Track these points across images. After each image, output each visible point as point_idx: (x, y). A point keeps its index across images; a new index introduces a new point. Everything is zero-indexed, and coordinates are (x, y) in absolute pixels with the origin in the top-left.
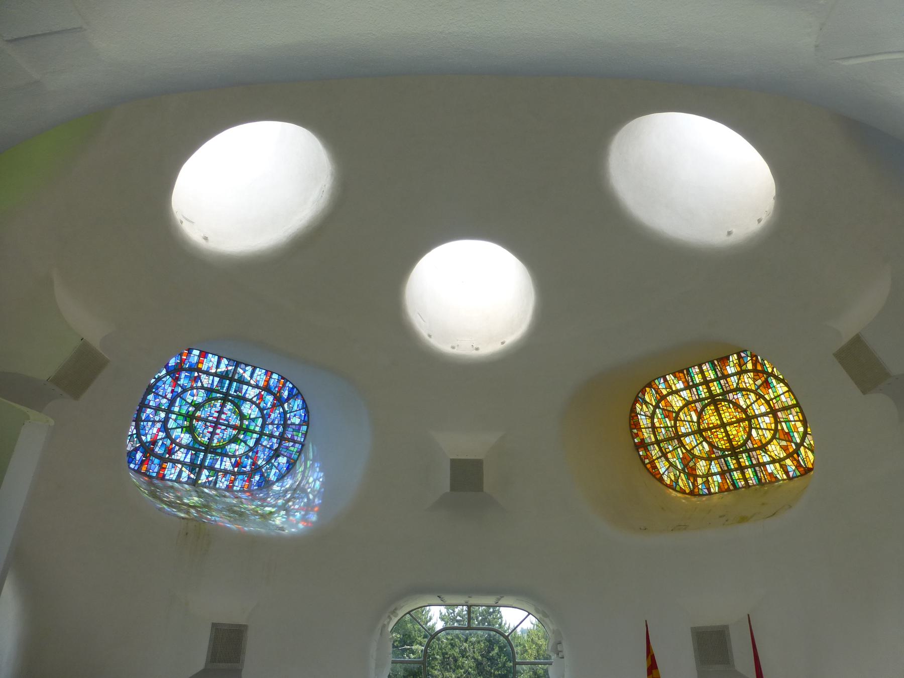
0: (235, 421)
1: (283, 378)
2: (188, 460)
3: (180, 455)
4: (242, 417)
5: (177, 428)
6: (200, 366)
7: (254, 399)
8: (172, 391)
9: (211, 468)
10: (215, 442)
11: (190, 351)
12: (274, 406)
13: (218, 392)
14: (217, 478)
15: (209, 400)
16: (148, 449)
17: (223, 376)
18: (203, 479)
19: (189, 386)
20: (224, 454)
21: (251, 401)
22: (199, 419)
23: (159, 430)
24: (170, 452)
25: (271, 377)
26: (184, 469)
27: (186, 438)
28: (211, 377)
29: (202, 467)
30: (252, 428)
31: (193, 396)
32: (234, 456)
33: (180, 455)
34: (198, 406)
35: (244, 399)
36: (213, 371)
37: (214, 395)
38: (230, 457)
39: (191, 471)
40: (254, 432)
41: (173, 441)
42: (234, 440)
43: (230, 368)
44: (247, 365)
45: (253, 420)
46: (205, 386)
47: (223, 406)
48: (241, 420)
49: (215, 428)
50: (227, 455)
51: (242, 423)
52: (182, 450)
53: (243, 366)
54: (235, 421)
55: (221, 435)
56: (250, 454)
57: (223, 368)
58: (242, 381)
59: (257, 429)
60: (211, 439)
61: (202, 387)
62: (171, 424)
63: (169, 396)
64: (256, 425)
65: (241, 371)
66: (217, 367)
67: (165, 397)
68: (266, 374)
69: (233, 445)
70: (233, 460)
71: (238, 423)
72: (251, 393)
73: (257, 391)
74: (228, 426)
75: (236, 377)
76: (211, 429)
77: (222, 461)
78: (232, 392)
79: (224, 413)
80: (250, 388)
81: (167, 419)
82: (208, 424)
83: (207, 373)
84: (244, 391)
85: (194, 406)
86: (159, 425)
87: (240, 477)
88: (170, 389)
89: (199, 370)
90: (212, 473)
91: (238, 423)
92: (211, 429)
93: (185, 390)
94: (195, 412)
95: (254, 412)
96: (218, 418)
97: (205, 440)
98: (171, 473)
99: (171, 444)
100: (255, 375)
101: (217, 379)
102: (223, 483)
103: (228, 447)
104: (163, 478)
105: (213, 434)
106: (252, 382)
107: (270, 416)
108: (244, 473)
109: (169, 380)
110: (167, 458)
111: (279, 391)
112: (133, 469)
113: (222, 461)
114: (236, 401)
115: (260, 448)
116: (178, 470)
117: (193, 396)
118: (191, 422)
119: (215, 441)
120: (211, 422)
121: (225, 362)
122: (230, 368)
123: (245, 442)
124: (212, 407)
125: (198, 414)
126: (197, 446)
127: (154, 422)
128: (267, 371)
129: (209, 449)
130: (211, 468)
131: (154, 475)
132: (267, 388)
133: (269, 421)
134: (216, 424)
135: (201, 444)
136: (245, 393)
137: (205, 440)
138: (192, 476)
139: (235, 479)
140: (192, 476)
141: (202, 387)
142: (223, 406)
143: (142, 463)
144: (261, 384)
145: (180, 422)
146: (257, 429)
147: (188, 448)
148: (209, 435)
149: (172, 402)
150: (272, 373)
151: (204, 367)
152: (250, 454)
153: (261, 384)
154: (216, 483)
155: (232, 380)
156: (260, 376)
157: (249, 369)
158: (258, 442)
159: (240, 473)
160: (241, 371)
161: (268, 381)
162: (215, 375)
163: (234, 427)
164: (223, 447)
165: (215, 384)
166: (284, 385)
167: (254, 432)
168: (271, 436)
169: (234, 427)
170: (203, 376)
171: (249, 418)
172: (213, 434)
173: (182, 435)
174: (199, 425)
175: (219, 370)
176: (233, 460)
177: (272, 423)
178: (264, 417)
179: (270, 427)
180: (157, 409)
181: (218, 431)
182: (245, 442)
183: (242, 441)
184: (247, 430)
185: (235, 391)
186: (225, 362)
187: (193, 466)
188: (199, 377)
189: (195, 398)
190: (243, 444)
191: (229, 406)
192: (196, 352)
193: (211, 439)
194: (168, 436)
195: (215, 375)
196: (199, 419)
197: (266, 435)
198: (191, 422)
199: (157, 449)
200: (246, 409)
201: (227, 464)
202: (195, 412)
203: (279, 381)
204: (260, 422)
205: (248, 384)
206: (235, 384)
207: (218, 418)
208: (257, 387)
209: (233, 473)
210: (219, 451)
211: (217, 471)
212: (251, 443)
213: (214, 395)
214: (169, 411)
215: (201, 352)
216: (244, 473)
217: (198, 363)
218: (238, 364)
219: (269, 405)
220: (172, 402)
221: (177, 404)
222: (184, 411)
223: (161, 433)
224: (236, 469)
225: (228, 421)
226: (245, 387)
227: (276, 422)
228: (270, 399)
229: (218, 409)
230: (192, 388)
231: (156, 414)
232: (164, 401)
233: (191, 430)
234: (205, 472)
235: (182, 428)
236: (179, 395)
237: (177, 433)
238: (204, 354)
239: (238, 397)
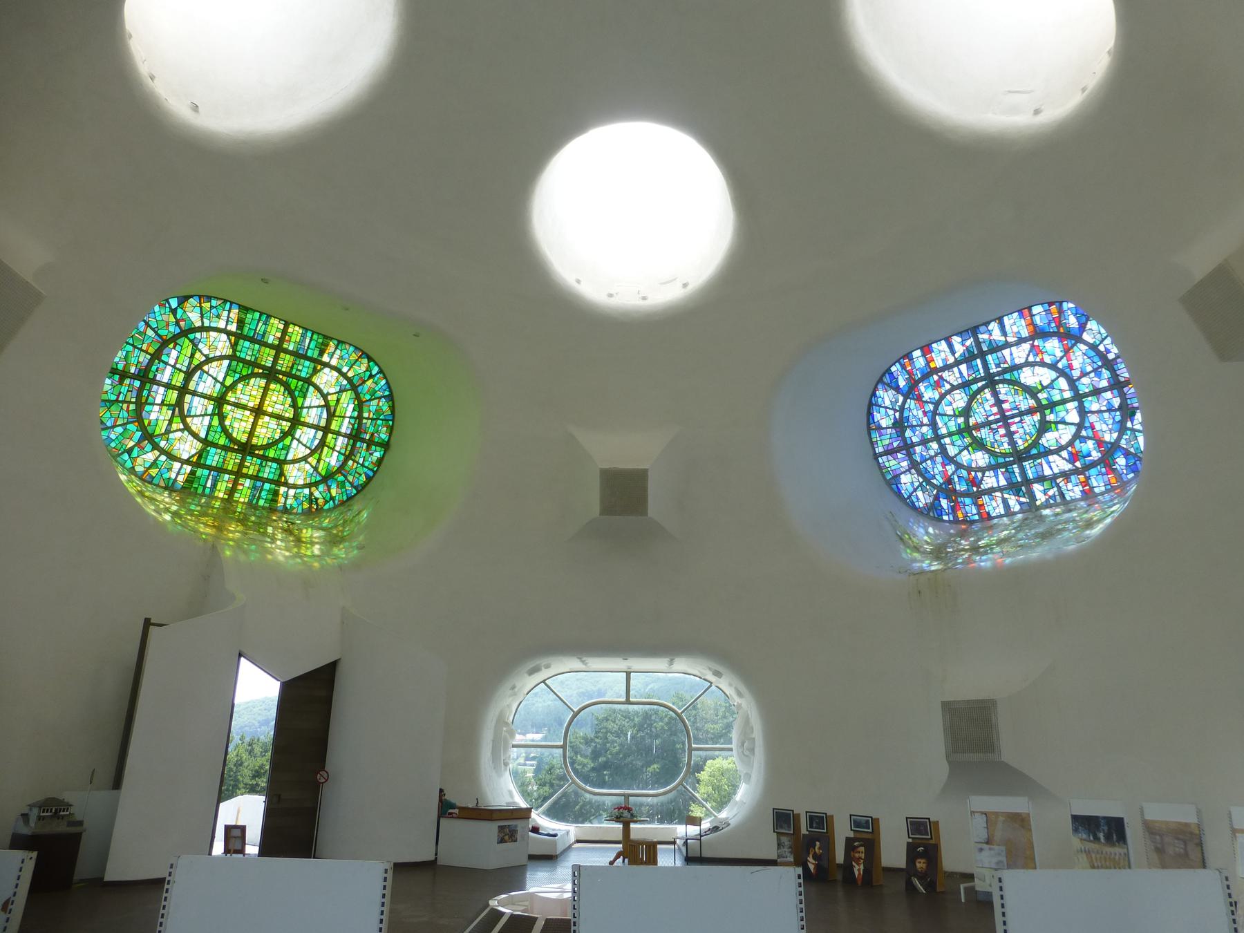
0: (1025, 403)
1: (1050, 304)
2: (1003, 482)
3: (989, 481)
4: (1031, 392)
5: (961, 452)
6: (932, 365)
7: (1031, 359)
8: (925, 413)
9: (1041, 479)
10: (1021, 445)
11: (908, 356)
12: (1067, 351)
13: (976, 381)
14: (1059, 488)
15: (972, 398)
16: (946, 488)
17: (968, 358)
18: (1041, 498)
19: (937, 396)
20: (1047, 453)
21: (1027, 364)
22: (978, 427)
23: (944, 465)
24: (974, 482)
25: (1032, 316)
26: (1006, 496)
27: (981, 459)
28: (955, 369)
29: (1028, 482)
30: (1057, 398)
31: (951, 404)
32: (1061, 448)
33: (989, 481)
34: (966, 412)
35: (1016, 367)
36: (951, 360)
37: (975, 387)
38: (1057, 451)
39: (1017, 494)
40: (1064, 402)
41: (969, 469)
42: (1044, 427)
43: (968, 343)
44: (987, 324)
45: (1051, 386)
46: (955, 383)
47: (995, 394)
49: (1007, 426)
50: (1051, 452)
51: (1038, 401)
52: (987, 473)
53: (982, 329)
54: (1025, 403)
55: (1021, 431)
56: (1084, 433)
57: (959, 349)
58: (996, 348)
59: (1068, 395)
60: (1013, 443)
61: (954, 388)
62: (952, 451)
63: (925, 420)
64: (1062, 391)
65: (986, 336)
66: (953, 352)
67: (922, 425)
68: (1022, 316)
69: (1048, 435)
70: (1064, 454)
71: (1032, 403)
72: (1020, 354)
73: (1026, 346)
74: (1021, 414)
75: (985, 349)
76: (1002, 431)
77: (1049, 463)
78: (993, 369)
79: (1003, 402)
80: (1014, 349)
81: (943, 449)
82: (994, 426)
83: (947, 367)
84: (1008, 358)
85: (960, 416)
86: (939, 459)
87: (1093, 471)
88: (920, 414)
89: (936, 371)
90: (1047, 484)
91: (1032, 403)
92: (1002, 431)
93: (937, 404)
94: (967, 421)
95: (1046, 375)
96: (1002, 411)
98: (994, 506)
99: (969, 474)
100: (1007, 328)
101: (963, 367)
102: (1073, 490)
103: (1043, 441)
104: (989, 517)
105: (1010, 435)
106: (1010, 339)
107: (1071, 367)
108: (1093, 464)
109: (911, 403)
110: (977, 493)
111: (1059, 325)
112: (949, 521)
113: (1049, 463)
114: (1007, 376)
116: (1000, 501)
117: (951, 404)
118: (971, 435)
119: (1020, 442)
120: (996, 421)
121: (956, 340)
122: (968, 343)
123: (1063, 422)
124: (982, 404)
125: (972, 421)
126: (1001, 460)
127: (931, 458)
128: (1020, 311)
129: (1020, 456)
130: (1041, 479)
131: (976, 517)
132: (1038, 334)
133: (1076, 374)
134: (1004, 419)
135: (1004, 455)
136: (1013, 360)
137: (1006, 447)
138: (1023, 500)
139: (1088, 478)
140: (1023, 500)
141: (954, 388)
142: (995, 394)
143: (954, 510)
144: (1025, 333)
145: (959, 443)
146: (1068, 395)
147: (993, 467)
149: (933, 425)
150: (1030, 309)
151: (938, 363)
152: (1084, 433)
153: (1025, 333)
154: (1062, 495)
155: (983, 355)
156: (1016, 325)
157: (994, 326)
158: (1082, 412)
159: (1087, 467)
160: (986, 336)
161: (1032, 323)
162: (957, 363)
163: (1031, 411)
164: (1035, 443)
165: (965, 374)
166: (1061, 311)
167: (1064, 402)
168: (1097, 392)
169: (1031, 411)
170: (945, 375)
171: (1044, 388)
172: (1010, 435)
173: (973, 457)
174: (984, 433)
175: (957, 355)
177: (1084, 374)
179: (1085, 380)
180: (924, 442)
181: (1013, 428)
182: (1063, 422)
183: (1057, 423)
184: (1052, 405)
185: (998, 366)
186: (956, 340)
187: (1014, 487)
188: (941, 377)
189: (955, 405)
190: (1060, 426)
191: (1003, 389)
192: (917, 353)
193: (1013, 443)
194: (959, 466)
195: (957, 363)
196: (978, 427)
197: (1087, 395)
198: (971, 435)
199: (958, 487)
200: (1028, 377)
201: (1059, 463)
202: (967, 421)
203: (1048, 312)
204: (1063, 383)
205: (1007, 345)
206: (989, 358)
207: (1002, 411)
208: (1021, 341)
209: (1076, 472)
210: (1034, 451)
211: (1053, 478)
212: (1074, 417)
213: (975, 387)
214: (938, 438)
215: (922, 348)
216: (1093, 464)
217: (928, 364)
218: (974, 331)
219: (1059, 354)
220: (933, 425)
221: (940, 424)
222: (953, 429)
223: (948, 467)
224: (1078, 464)
226: (1006, 352)
227: (1089, 369)
228: (1053, 347)
229: (992, 401)
230: (942, 396)
231: (928, 450)
232: (925, 429)
233: (979, 445)
234: (1037, 488)
235: (966, 448)
236: (935, 413)
237: (965, 458)
238: (927, 350)
239: (1005, 371)
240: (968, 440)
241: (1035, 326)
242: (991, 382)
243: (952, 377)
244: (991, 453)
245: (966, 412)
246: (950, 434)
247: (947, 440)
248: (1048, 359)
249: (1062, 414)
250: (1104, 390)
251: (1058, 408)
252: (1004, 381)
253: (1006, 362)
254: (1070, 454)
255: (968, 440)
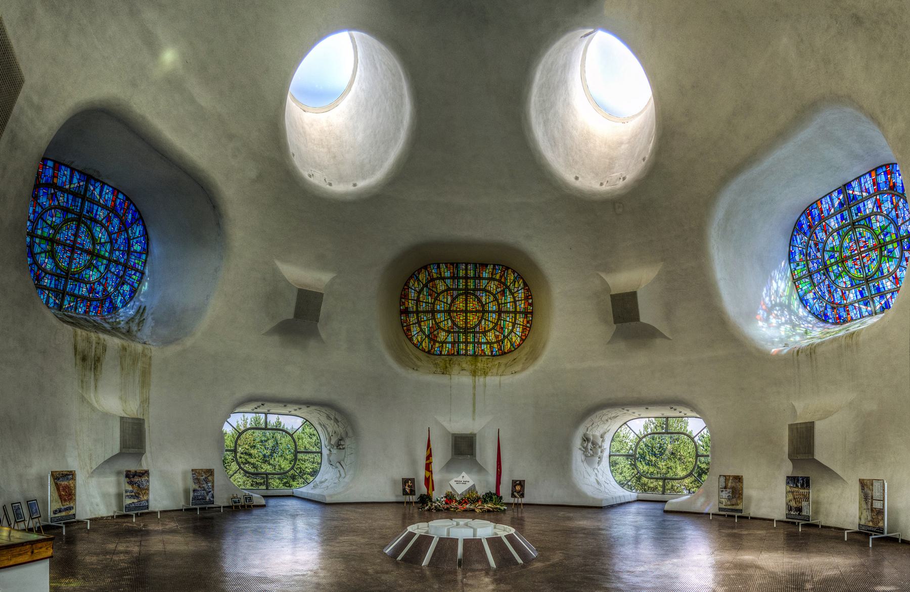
2: (52, 286)
4: (93, 239)
8: (34, 212)
13: (72, 212)
15: (66, 221)
17: (75, 194)
38: (86, 283)
42: (88, 267)
45: (103, 244)
47: (78, 228)
48: (94, 244)
49: (73, 252)
53: (93, 182)
54: (88, 246)
58: (93, 202)
60: (69, 264)
62: (37, 249)
69: (88, 271)
70: (88, 286)
72: (101, 214)
76: (69, 254)
85: (53, 228)
92: (69, 254)
95: (102, 236)
96: (75, 241)
97: (64, 265)
107: (117, 240)
111: (124, 214)
114: (88, 222)
115: (109, 275)
118: (52, 246)
119: (74, 266)
120: (69, 246)
123: (97, 269)
125: (58, 237)
133: (116, 246)
134: (73, 248)
142: (78, 228)
144: (110, 204)
145: (44, 246)
148: (67, 259)
162: (69, 192)
176: (88, 286)
177: (119, 250)
178: (112, 242)
182: (97, 269)
184: (98, 256)
185: (88, 212)
198: (52, 246)
201: (84, 291)
204: (108, 247)
210: (76, 276)
211: (77, 297)
213: (70, 216)
219: (116, 230)
222: (45, 235)
225: (82, 245)
226: (95, 207)
233: (52, 255)
234: (67, 298)
239: (91, 219)
240: (49, 248)
241: (115, 205)
242: (79, 219)
243: (62, 199)
244: (57, 265)
245: (57, 229)
246: (42, 237)
247: (37, 240)
248: (111, 228)
249: (99, 264)
250: (120, 263)
251: (100, 259)
252: (86, 225)
253: (92, 213)
254: (91, 288)
255: (49, 248)
